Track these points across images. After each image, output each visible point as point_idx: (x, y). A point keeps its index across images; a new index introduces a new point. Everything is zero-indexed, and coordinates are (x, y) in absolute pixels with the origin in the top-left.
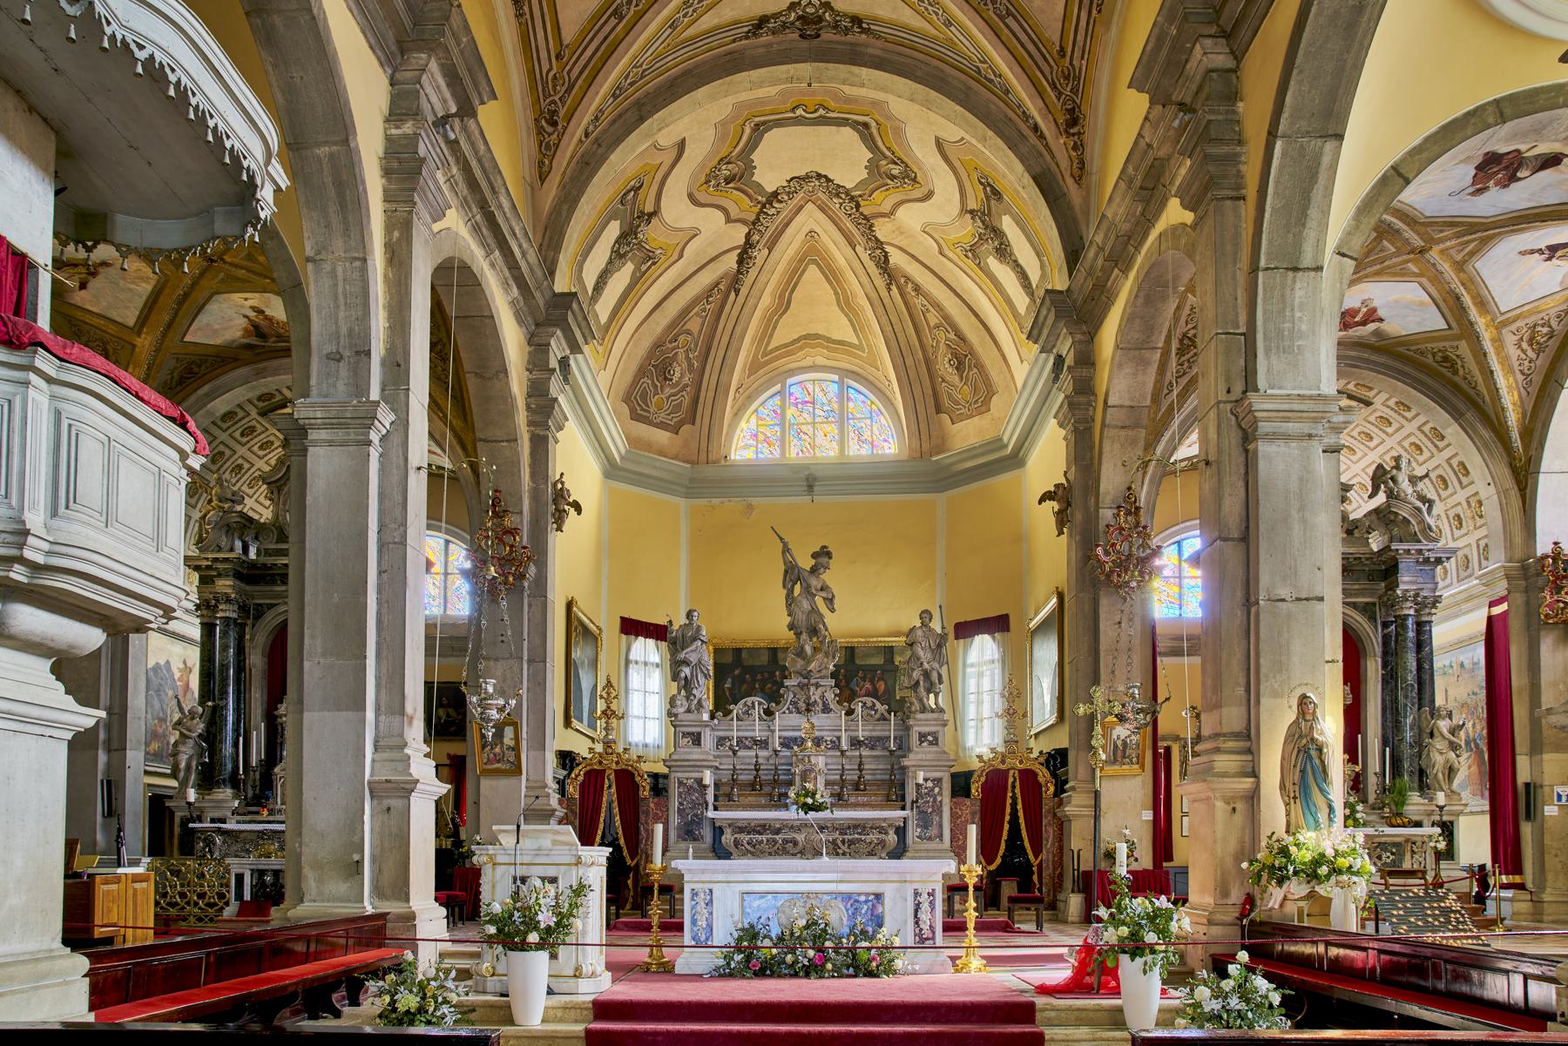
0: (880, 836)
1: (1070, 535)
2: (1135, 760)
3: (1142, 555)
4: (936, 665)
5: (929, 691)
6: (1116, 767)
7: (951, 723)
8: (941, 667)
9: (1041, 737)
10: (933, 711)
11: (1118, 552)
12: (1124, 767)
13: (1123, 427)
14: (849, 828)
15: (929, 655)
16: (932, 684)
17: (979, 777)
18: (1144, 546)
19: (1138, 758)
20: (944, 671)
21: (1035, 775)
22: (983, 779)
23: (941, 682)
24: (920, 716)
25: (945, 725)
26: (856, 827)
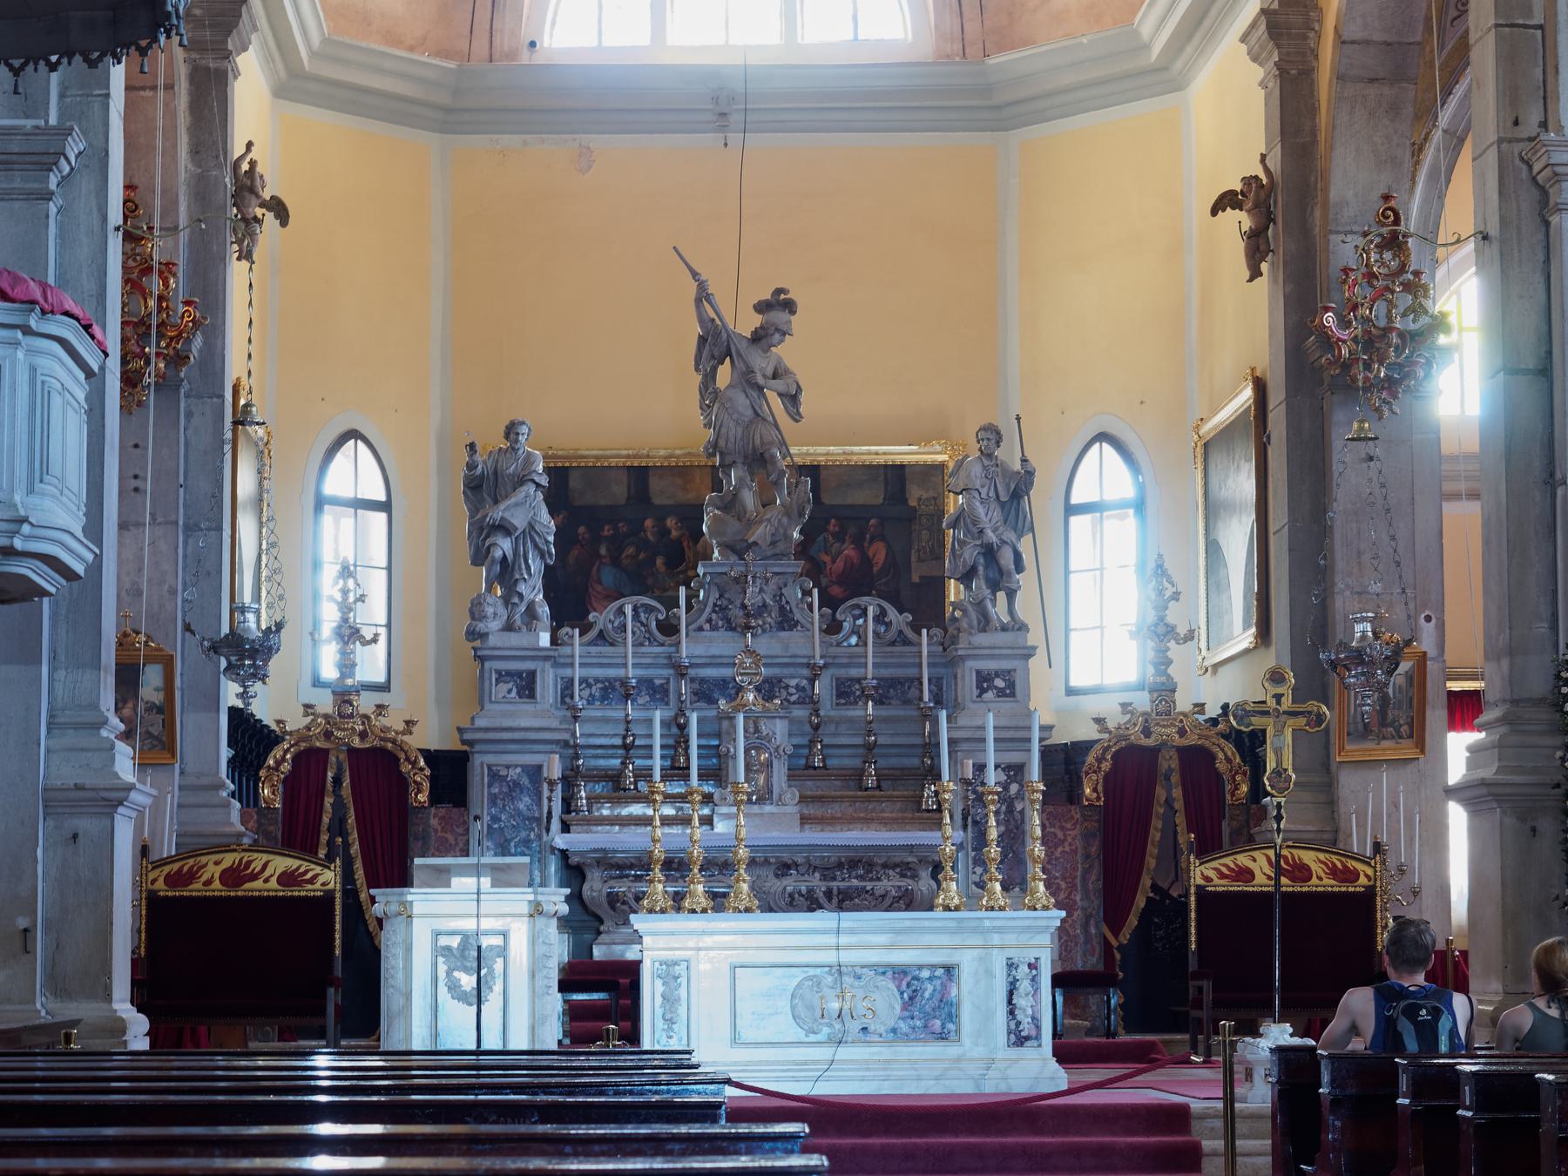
0: (903, 883)
1: (1273, 280)
2: (1404, 729)
3: (1412, 327)
4: (1010, 536)
5: (995, 586)
6: (1370, 745)
7: (1041, 654)
8: (1019, 537)
9: (1221, 670)
10: (1004, 628)
11: (1367, 320)
12: (1385, 744)
13: (1372, 81)
14: (840, 866)
15: (997, 515)
16: (1001, 571)
17: (1100, 760)
18: (1417, 310)
19: (1411, 725)
20: (1025, 545)
21: (1213, 757)
22: (1106, 766)
23: (1019, 567)
24: (981, 639)
25: (1028, 657)
26: (853, 864)
